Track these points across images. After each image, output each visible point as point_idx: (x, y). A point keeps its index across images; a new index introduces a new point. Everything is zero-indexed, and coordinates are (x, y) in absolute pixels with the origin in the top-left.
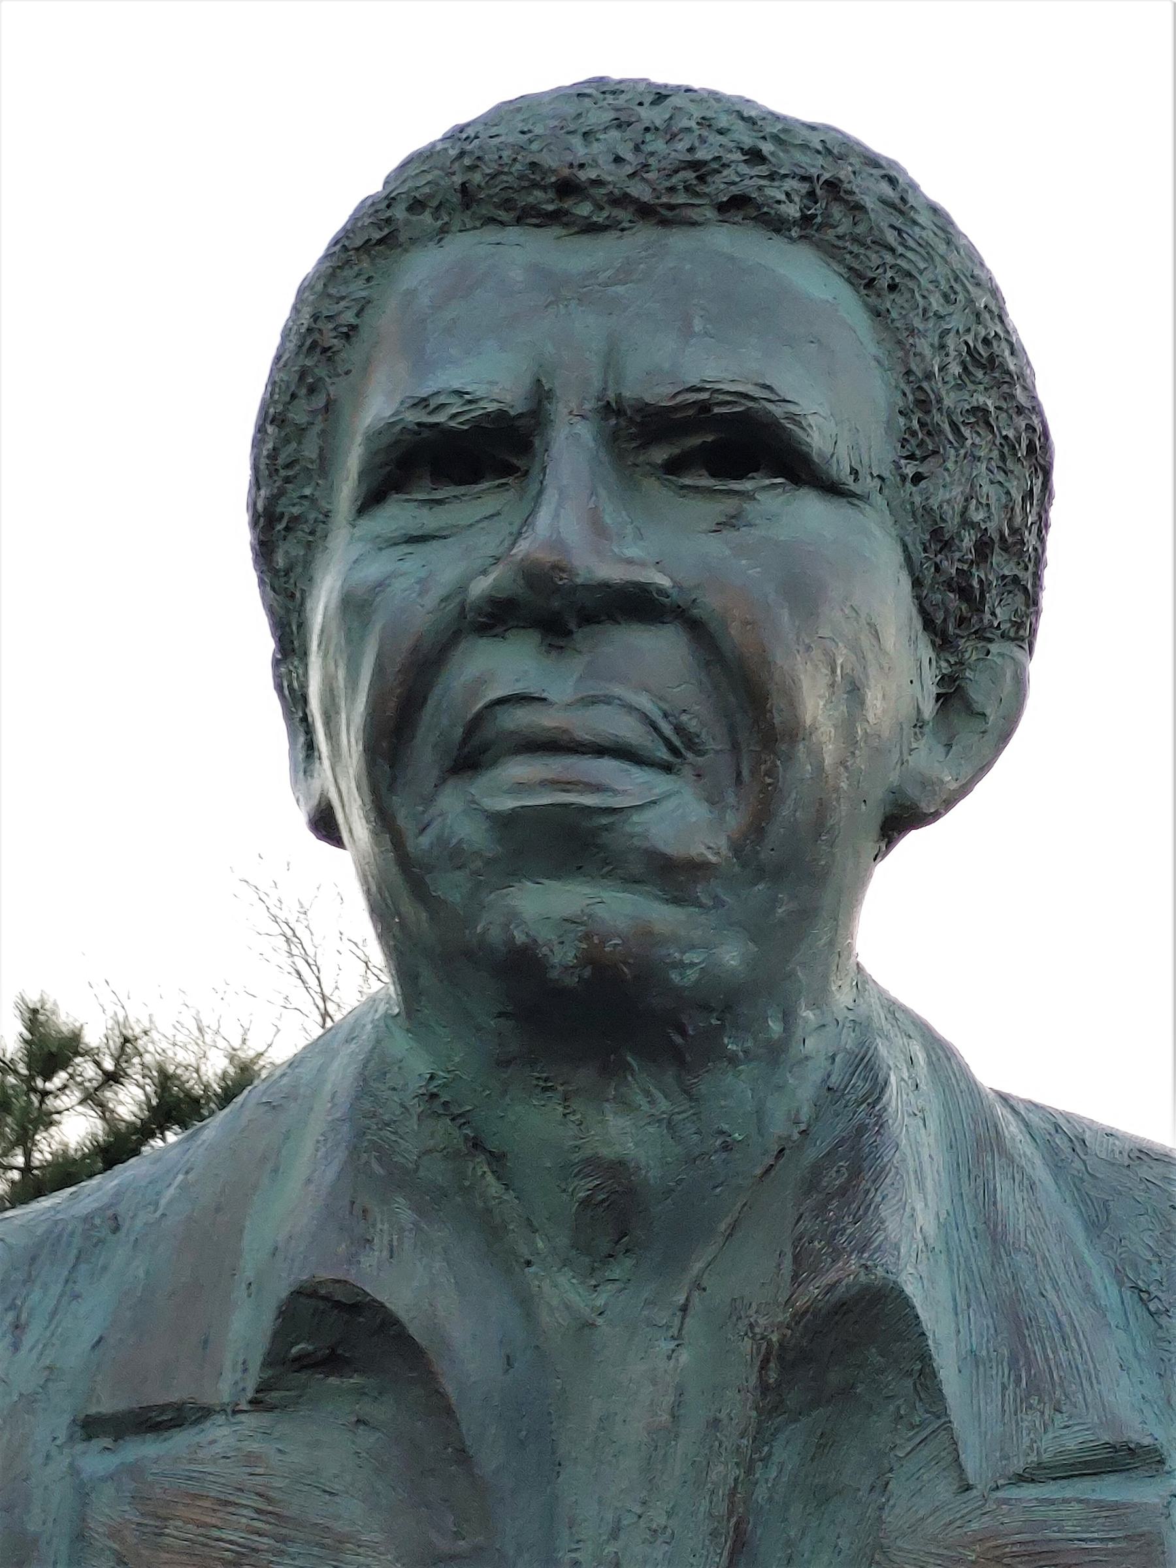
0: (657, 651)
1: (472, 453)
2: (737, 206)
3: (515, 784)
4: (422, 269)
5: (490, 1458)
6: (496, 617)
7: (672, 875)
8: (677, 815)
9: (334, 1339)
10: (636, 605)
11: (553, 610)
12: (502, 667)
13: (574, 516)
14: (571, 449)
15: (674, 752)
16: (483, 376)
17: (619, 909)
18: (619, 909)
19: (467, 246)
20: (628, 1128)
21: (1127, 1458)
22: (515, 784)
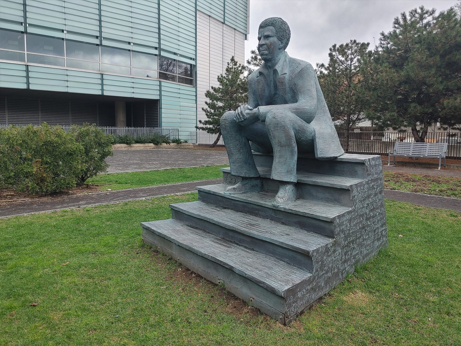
0: (265, 46)
5: (267, 76)
7: (266, 55)
20: (269, 64)
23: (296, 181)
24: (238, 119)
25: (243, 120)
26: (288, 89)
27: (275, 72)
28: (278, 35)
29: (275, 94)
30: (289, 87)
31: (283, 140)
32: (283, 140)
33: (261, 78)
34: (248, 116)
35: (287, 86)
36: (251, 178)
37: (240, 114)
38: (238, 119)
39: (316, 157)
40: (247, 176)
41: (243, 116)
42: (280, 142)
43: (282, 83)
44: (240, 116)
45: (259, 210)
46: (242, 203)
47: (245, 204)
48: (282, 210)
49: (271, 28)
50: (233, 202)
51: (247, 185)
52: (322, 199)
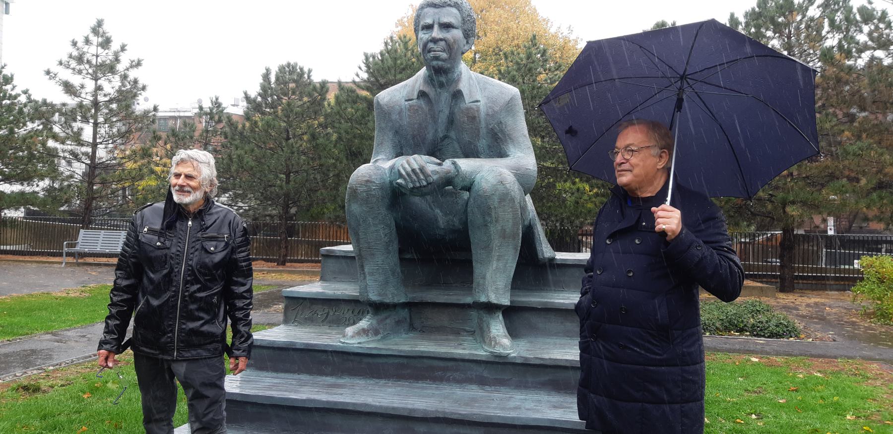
0: (443, 43)
1: (429, 27)
2: (450, 5)
3: (432, 54)
4: (426, 10)
6: (431, 41)
7: (444, 60)
8: (444, 55)
9: (422, 94)
10: (441, 40)
11: (435, 41)
12: (431, 45)
13: (436, 33)
14: (436, 27)
15: (444, 51)
16: (429, 21)
17: (440, 63)
18: (440, 63)
19: (428, 9)
20: (443, 79)
21: (477, 101)
22: (432, 54)
23: (509, 304)
24: (413, 182)
25: (425, 183)
26: (483, 131)
27: (458, 95)
28: (465, 27)
29: (446, 137)
30: (487, 127)
31: (509, 226)
32: (509, 226)
33: (422, 102)
34: (435, 177)
35: (483, 124)
36: (395, 306)
37: (418, 171)
38: (413, 182)
39: (540, 257)
40: (396, 301)
41: (426, 176)
42: (503, 230)
43: (474, 118)
44: (418, 177)
45: (445, 369)
46: (397, 361)
47: (405, 361)
48: (518, 361)
49: (454, 10)
50: (366, 360)
51: (388, 321)
52: (557, 334)
